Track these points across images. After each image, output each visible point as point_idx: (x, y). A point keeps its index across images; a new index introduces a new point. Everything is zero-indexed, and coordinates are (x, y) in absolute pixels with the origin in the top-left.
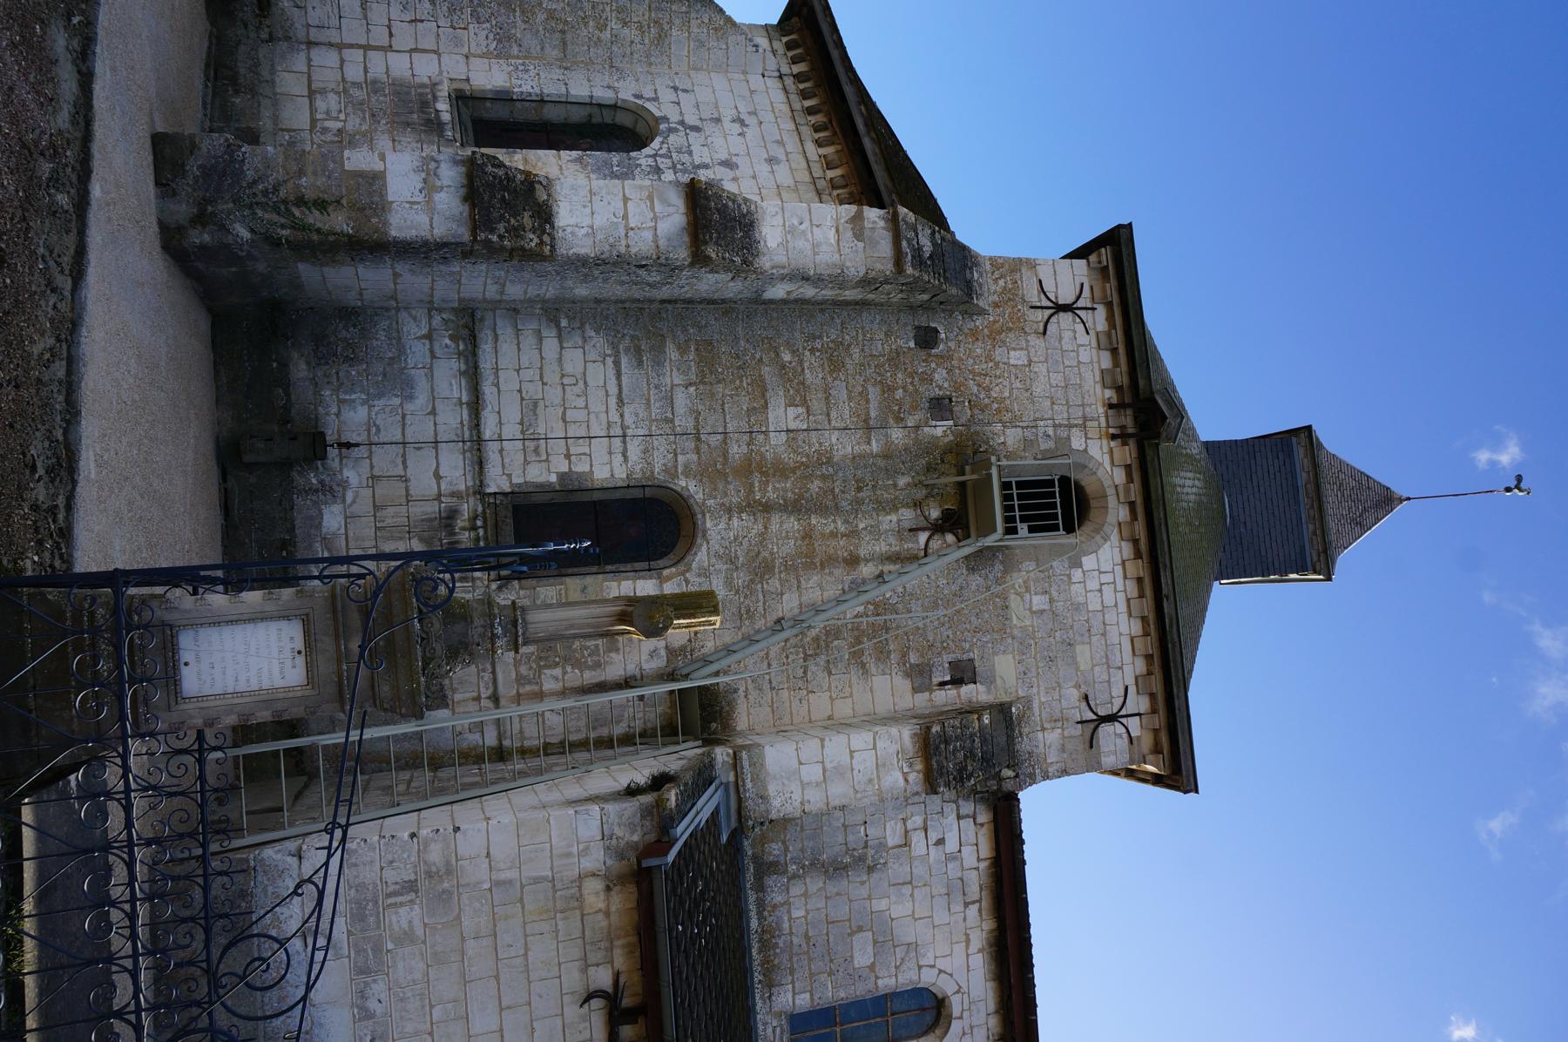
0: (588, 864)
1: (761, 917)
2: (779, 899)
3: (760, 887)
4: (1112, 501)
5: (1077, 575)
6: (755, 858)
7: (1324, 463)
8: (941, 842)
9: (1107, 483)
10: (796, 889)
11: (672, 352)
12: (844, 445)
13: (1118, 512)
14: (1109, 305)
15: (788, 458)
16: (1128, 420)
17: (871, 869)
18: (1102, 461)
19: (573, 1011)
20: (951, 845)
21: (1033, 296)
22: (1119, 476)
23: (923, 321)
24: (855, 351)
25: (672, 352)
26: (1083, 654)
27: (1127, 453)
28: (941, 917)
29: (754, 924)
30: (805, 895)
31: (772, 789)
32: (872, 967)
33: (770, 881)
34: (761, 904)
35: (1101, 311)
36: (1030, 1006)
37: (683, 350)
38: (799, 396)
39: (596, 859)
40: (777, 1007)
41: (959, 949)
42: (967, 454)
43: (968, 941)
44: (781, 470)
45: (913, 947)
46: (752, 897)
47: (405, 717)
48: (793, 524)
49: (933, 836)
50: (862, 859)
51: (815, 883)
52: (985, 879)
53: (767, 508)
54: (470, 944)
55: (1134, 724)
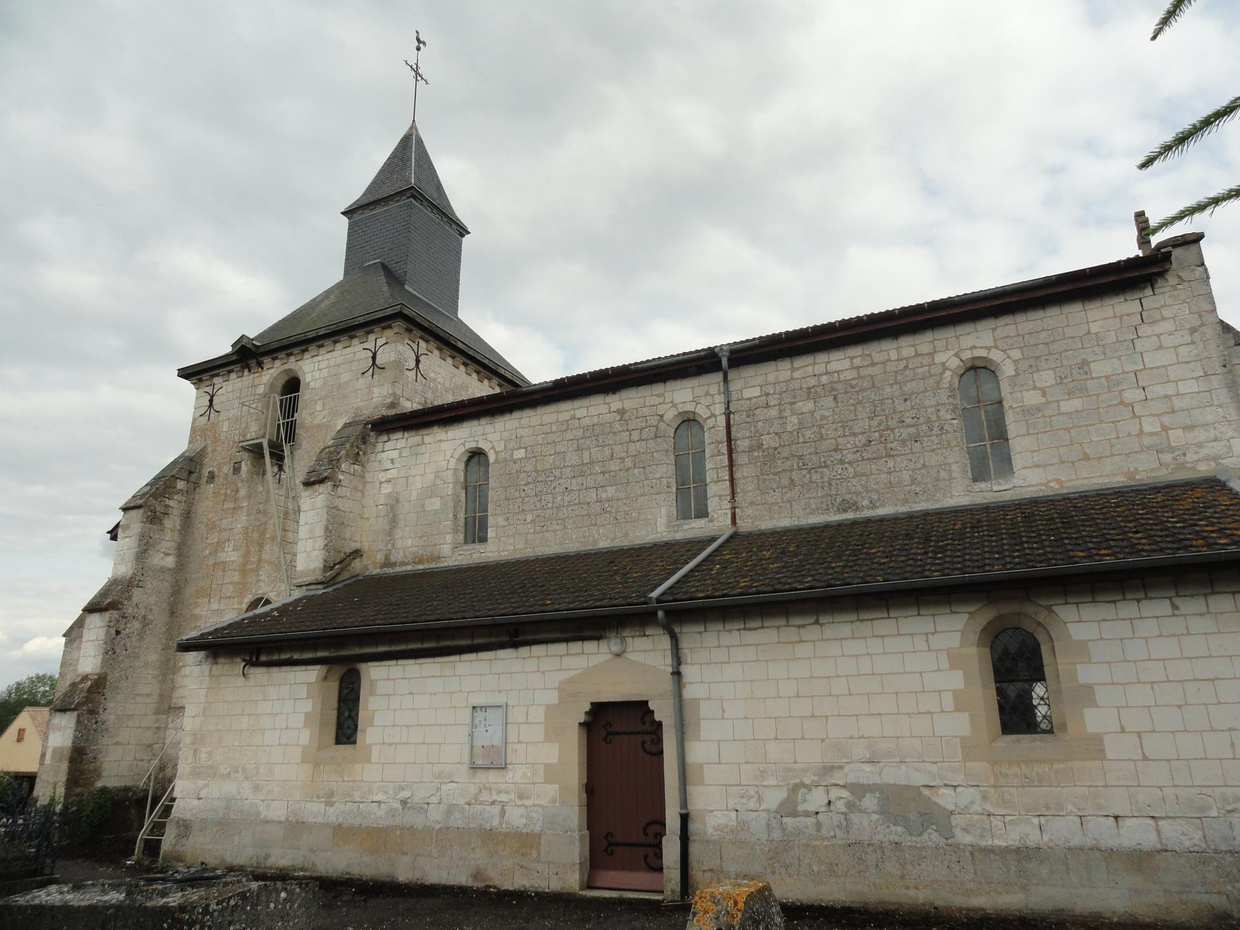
0: (207, 672)
1: (408, 564)
2: (401, 554)
3: (394, 565)
4: (287, 367)
5: (312, 385)
6: (382, 567)
7: (387, 191)
8: (392, 461)
9: (280, 370)
10: (399, 544)
11: (197, 611)
12: (241, 521)
13: (292, 364)
14: (213, 376)
15: (242, 551)
16: (253, 363)
17: (398, 501)
18: (271, 373)
19: (252, 681)
20: (395, 454)
21: (205, 418)
22: (278, 363)
23: (204, 480)
24: (211, 515)
25: (197, 611)
26: (345, 377)
27: (267, 361)
28: (426, 458)
29: (409, 568)
30: (402, 538)
31: (312, 567)
32: (442, 498)
33: (393, 559)
34: (403, 564)
35: (216, 380)
36: (461, 405)
37: (197, 605)
38: (219, 545)
39: (206, 668)
40: (449, 554)
41: (443, 446)
42: (256, 451)
43: (441, 441)
44: (247, 555)
45: (437, 474)
46: (398, 569)
47: (659, 741)
48: (267, 548)
49: (390, 466)
50: (392, 507)
51: (399, 534)
52: (413, 433)
53: (260, 561)
54: (220, 727)
55: (380, 342)
